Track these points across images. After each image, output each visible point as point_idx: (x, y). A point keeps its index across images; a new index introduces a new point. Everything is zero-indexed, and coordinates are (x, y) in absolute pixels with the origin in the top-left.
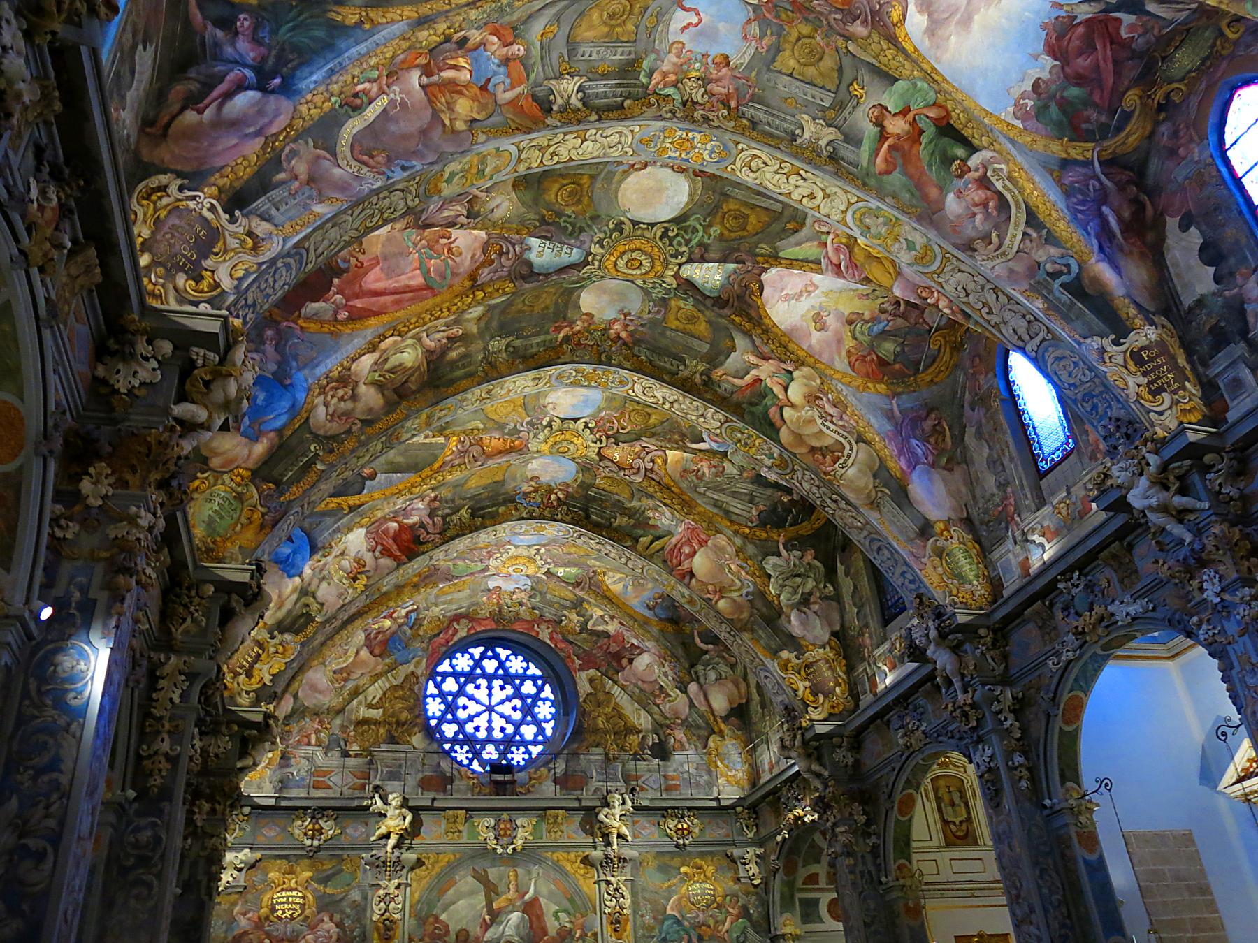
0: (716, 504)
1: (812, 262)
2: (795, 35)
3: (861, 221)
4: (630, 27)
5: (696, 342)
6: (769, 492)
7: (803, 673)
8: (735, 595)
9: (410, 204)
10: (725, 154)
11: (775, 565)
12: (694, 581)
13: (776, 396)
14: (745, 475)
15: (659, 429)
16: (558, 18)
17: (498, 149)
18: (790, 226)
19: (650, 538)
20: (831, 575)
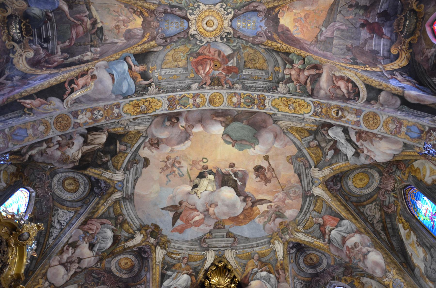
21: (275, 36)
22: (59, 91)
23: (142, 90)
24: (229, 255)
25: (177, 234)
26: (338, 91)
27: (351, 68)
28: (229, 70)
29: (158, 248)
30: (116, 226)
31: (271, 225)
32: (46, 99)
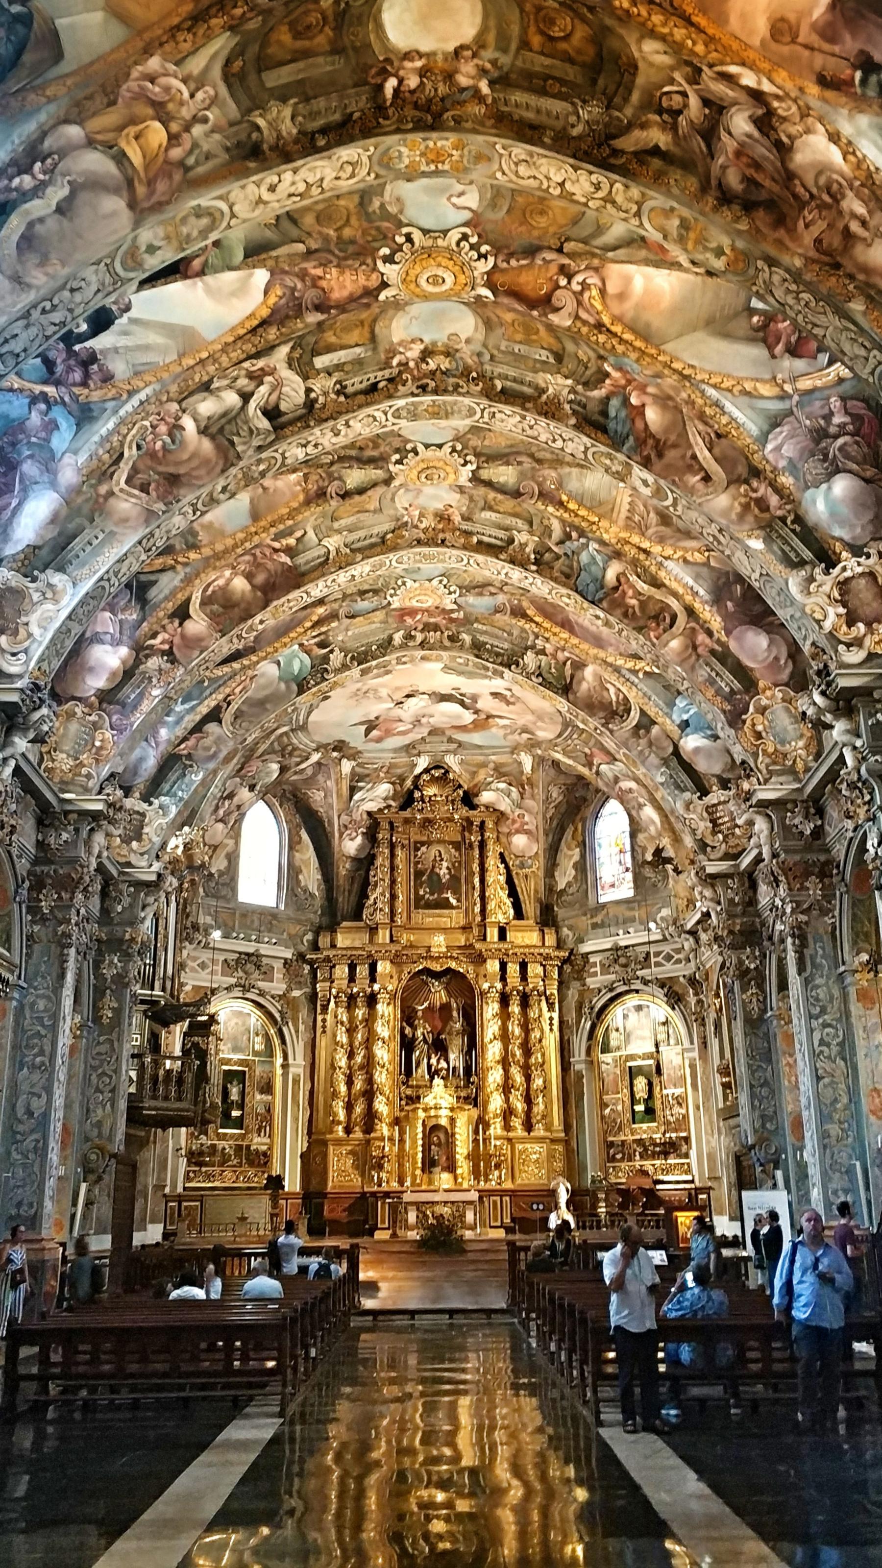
2: (354, 221)
3: (210, 214)
4: (520, 199)
9: (766, 268)
10: (385, 161)
16: (600, 230)
17: (665, 237)
18: (238, 64)
21: (525, 604)
22: (214, 716)
23: (321, 668)
24: (451, 761)
25: (372, 746)
26: (605, 693)
27: (630, 670)
28: (452, 620)
29: (344, 761)
30: (283, 756)
31: (516, 737)
32: (200, 731)
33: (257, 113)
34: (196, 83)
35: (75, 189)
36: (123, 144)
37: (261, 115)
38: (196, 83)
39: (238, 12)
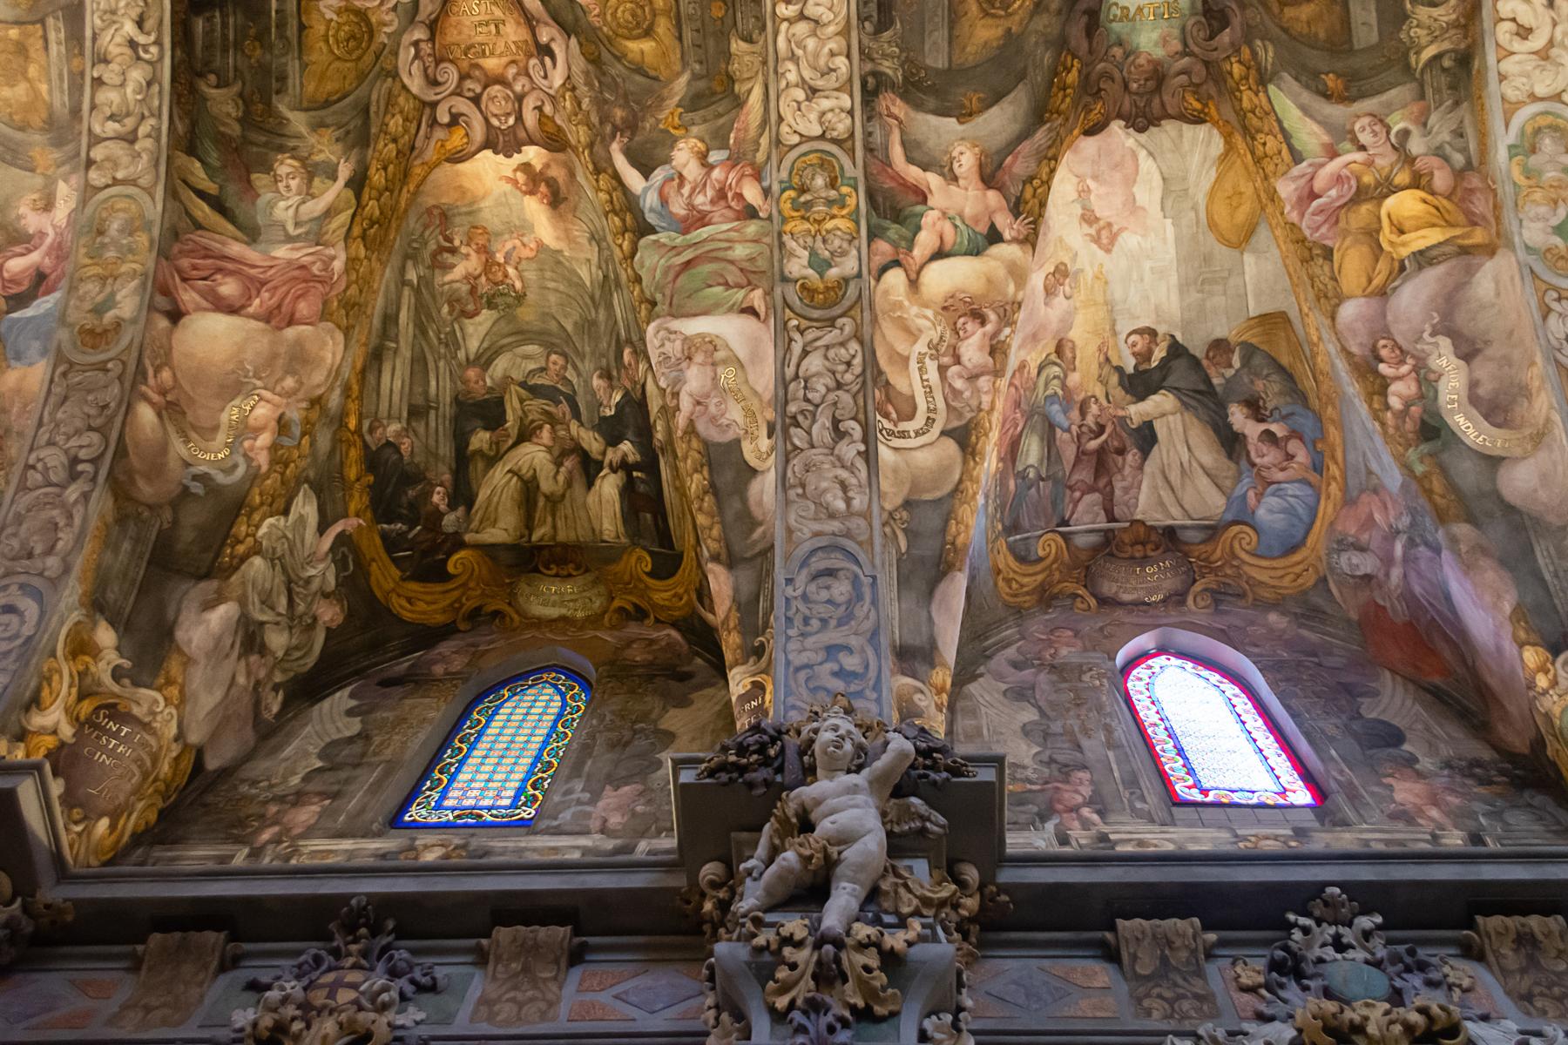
0: (390, 319)
1: (1291, 148)
3: (1538, 131)
5: (941, 36)
6: (446, 449)
7: (86, 707)
8: (178, 448)
11: (302, 519)
12: (163, 323)
13: (911, 244)
14: (472, 373)
15: (616, 69)
18: (1330, 81)
19: (211, 188)
20: (307, 689)
33: (1413, 59)
34: (1341, 137)
35: (1447, 328)
36: (1405, 252)
37: (1418, 53)
38: (1341, 137)
39: (1237, 70)
